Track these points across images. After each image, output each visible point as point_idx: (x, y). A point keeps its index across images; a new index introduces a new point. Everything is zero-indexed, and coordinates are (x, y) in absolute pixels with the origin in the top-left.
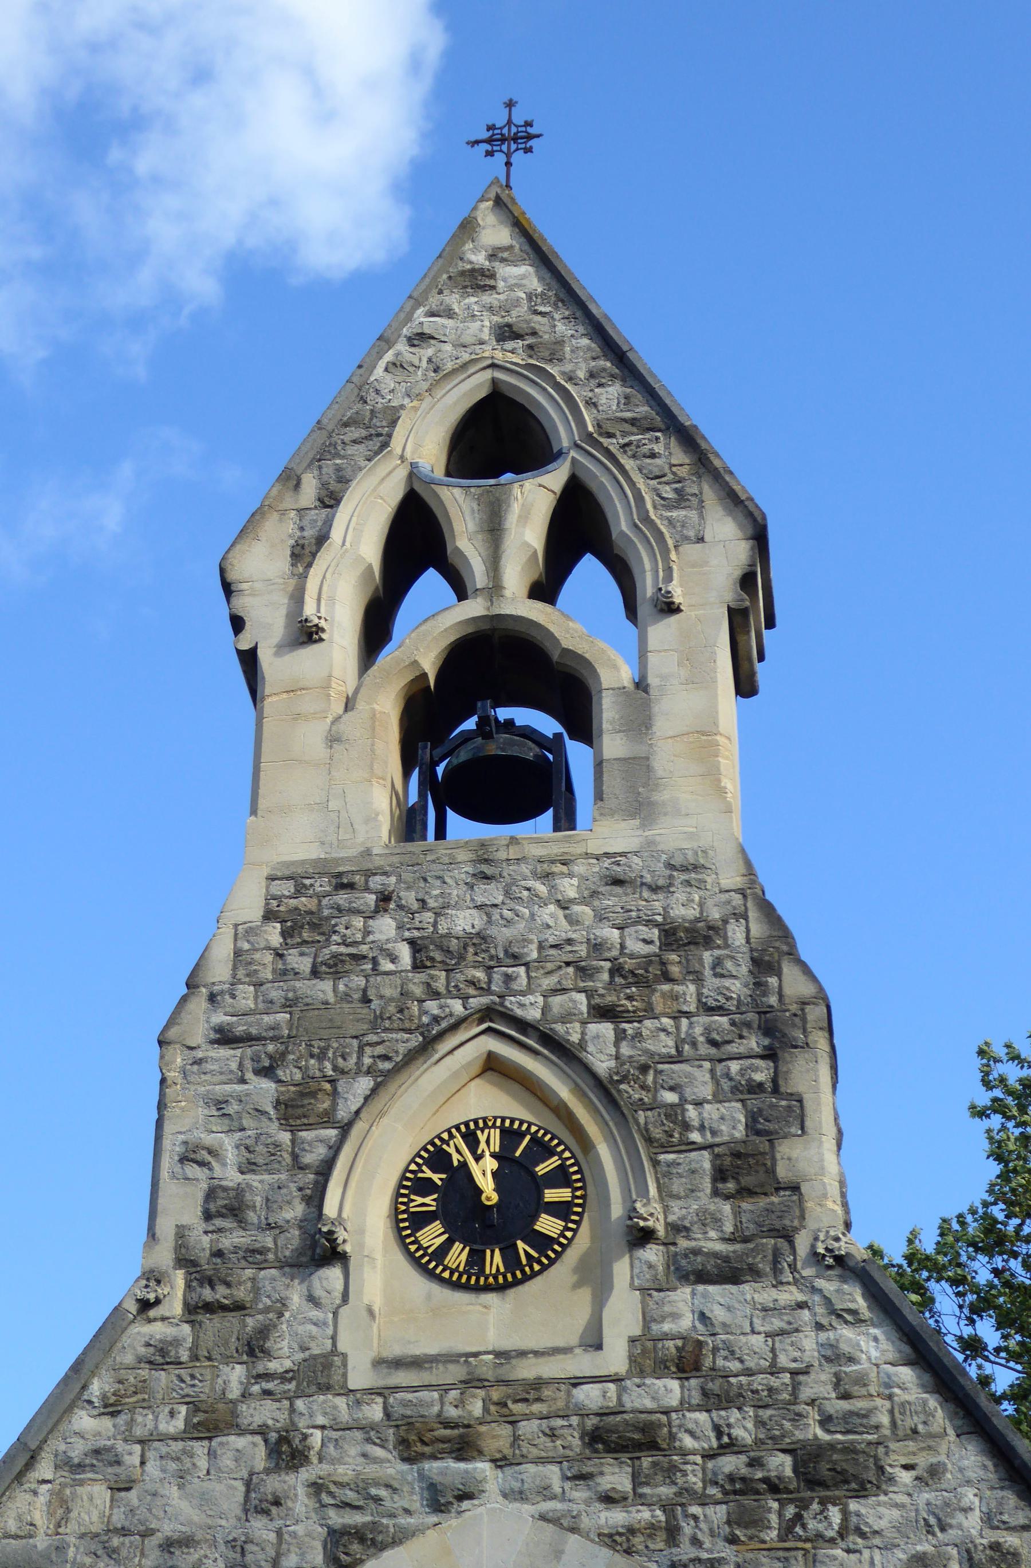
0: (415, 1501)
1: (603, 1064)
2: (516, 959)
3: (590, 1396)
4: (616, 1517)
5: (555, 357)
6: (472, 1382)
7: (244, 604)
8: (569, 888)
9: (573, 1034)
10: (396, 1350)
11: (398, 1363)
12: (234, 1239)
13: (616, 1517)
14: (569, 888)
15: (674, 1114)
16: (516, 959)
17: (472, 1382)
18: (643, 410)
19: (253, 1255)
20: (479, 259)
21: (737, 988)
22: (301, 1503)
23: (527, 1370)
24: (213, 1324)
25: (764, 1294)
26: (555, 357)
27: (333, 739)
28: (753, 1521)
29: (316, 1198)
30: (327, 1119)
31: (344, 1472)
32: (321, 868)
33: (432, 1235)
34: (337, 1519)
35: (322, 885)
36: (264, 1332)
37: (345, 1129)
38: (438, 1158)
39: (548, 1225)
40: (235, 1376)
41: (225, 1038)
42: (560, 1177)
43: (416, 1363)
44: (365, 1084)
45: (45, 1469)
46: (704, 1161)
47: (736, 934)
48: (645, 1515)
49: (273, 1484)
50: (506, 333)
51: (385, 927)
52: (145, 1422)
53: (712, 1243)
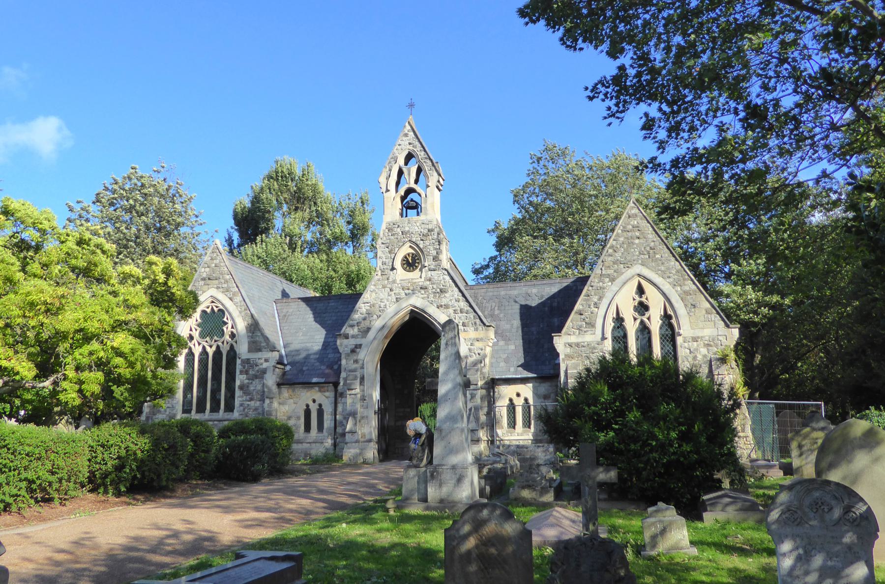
1: (421, 246)
3: (420, 283)
5: (416, 148)
8: (418, 224)
9: (418, 243)
14: (418, 224)
15: (429, 252)
19: (387, 269)
20: (406, 132)
21: (435, 237)
22: (393, 295)
23: (414, 281)
28: (436, 296)
29: (393, 263)
33: (405, 266)
38: (406, 257)
39: (417, 265)
41: (383, 244)
42: (418, 259)
49: (391, 293)
50: (410, 144)
51: (399, 229)
53: (432, 267)
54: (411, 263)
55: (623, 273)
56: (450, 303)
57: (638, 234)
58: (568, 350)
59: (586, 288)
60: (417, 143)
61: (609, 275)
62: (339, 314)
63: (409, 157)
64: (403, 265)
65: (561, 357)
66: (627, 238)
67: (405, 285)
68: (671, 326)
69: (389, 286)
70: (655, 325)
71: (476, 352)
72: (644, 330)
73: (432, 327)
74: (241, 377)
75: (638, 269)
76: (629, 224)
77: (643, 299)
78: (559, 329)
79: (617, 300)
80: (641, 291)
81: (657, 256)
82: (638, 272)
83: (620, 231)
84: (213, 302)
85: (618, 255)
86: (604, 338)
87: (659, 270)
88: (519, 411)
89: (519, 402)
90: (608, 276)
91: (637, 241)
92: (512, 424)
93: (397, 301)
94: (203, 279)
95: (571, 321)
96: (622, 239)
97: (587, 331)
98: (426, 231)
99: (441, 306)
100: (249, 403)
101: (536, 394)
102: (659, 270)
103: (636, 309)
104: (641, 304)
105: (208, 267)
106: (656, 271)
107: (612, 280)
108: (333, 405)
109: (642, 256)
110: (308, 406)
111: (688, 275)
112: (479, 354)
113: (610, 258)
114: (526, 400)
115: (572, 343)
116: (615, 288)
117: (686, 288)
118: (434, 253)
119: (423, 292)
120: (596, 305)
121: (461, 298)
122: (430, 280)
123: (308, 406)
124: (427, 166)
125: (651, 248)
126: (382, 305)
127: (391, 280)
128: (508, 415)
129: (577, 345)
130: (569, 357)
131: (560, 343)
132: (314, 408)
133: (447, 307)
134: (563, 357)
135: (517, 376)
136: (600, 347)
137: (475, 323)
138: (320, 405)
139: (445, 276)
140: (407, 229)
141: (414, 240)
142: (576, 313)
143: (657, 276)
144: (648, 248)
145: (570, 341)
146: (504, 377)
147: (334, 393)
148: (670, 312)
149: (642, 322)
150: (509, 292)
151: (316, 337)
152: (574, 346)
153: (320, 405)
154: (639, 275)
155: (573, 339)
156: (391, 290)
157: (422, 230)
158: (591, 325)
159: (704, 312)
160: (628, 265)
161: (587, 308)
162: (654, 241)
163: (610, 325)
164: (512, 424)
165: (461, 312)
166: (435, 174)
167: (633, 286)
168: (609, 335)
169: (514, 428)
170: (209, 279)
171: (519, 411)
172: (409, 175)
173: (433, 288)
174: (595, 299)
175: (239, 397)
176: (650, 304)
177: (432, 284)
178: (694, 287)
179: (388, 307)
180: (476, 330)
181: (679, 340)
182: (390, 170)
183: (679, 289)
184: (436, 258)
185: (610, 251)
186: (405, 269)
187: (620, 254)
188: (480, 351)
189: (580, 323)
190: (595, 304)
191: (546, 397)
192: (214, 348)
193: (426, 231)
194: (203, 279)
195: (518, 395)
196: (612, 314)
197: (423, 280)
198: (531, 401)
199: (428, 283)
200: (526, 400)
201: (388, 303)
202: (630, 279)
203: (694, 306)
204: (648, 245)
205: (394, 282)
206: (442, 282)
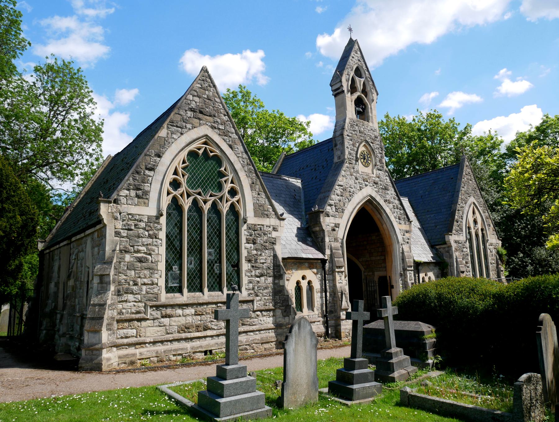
10: (363, 171)
11: (363, 173)
22: (358, 184)
34: (361, 186)
40: (352, 170)
51: (357, 127)
65: (454, 249)
74: (248, 246)
84: (205, 143)
94: (192, 110)
100: (258, 279)
105: (199, 97)
112: (408, 242)
122: (379, 178)
123: (298, 283)
126: (352, 190)
132: (304, 284)
138: (309, 283)
153: (309, 283)
156: (357, 179)
170: (201, 112)
175: (247, 271)
177: (380, 181)
188: (408, 241)
192: (209, 205)
194: (192, 110)
197: (374, 176)
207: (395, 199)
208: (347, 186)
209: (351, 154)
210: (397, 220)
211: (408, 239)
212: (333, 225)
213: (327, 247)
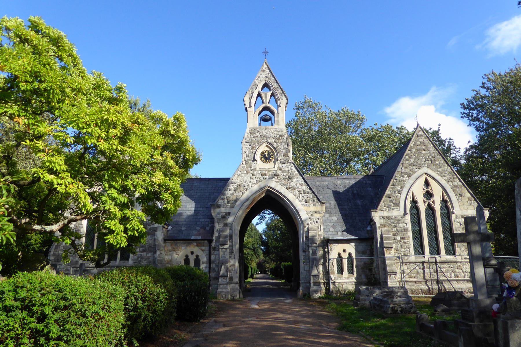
0: (262, 179)
1: (275, 146)
2: (268, 137)
3: (274, 172)
4: (276, 180)
5: (271, 80)
6: (266, 170)
7: (245, 103)
8: (273, 131)
9: (273, 144)
11: (261, 169)
12: (248, 159)
13: (276, 180)
14: (273, 131)
15: (280, 150)
16: (268, 137)
17: (266, 170)
18: (278, 86)
19: (250, 160)
20: (264, 69)
21: (285, 140)
22: (254, 178)
23: (270, 170)
24: (247, 165)
25: (287, 165)
26: (271, 80)
27: (254, 116)
29: (254, 156)
30: (255, 150)
31: (257, 176)
32: (253, 128)
33: (263, 159)
35: (253, 130)
36: (251, 166)
37: (256, 151)
38: (263, 153)
41: (246, 142)
43: (262, 169)
44: (257, 147)
45: (236, 175)
46: (282, 154)
47: (285, 136)
48: (278, 180)
50: (266, 77)
51: (258, 134)
52: (243, 172)
53: (283, 161)
54: (266, 158)
55: (416, 172)
56: (296, 186)
57: (424, 147)
58: (382, 221)
59: (392, 180)
60: (272, 77)
61: (406, 172)
62: (202, 191)
63: (266, 85)
64: (261, 158)
65: (378, 225)
66: (417, 150)
67: (263, 172)
68: (447, 207)
69: (251, 172)
70: (437, 207)
71: (315, 221)
72: (430, 209)
73: (282, 202)
75: (425, 170)
76: (418, 141)
77: (429, 189)
78: (375, 205)
79: (413, 189)
80: (427, 184)
81: (437, 162)
82: (425, 172)
83: (412, 145)
85: (412, 160)
86: (405, 214)
87: (438, 171)
88: (345, 262)
89: (345, 256)
90: (406, 173)
91: (424, 152)
92: (340, 271)
93: (257, 183)
95: (383, 202)
96: (414, 150)
97: (394, 209)
98: (278, 136)
99: (289, 188)
100: (142, 253)
101: (356, 250)
102: (438, 171)
103: (424, 196)
104: (428, 192)
106: (437, 172)
107: (409, 176)
108: (208, 256)
109: (427, 162)
110: (187, 256)
111: (456, 176)
112: (317, 222)
113: (407, 162)
114: (350, 254)
115: (384, 216)
116: (411, 181)
117: (456, 184)
118: (284, 151)
119: (276, 177)
120: (400, 192)
121: (304, 183)
122: (281, 170)
124: (279, 93)
125: (432, 157)
126: (246, 185)
127: (253, 168)
128: (337, 265)
129: (388, 218)
130: (382, 225)
131: (377, 216)
133: (293, 188)
134: (379, 225)
135: (345, 238)
136: (403, 219)
137: (314, 201)
138: (197, 256)
139: (292, 168)
140: (264, 134)
141: (270, 141)
142: (386, 196)
143: (437, 175)
144: (431, 157)
145: (383, 215)
146: (335, 238)
147: (208, 247)
148: (446, 198)
149: (429, 205)
150: (322, 183)
151: (188, 207)
152: (385, 218)
153: (197, 256)
154: (426, 174)
155: (385, 214)
156: (253, 175)
157: (276, 135)
158: (397, 205)
159: (467, 199)
160: (419, 167)
161: (393, 194)
162: (434, 153)
163: (409, 206)
164: (340, 271)
165: (304, 193)
166: (285, 99)
167: (422, 180)
168: (408, 211)
169: (342, 274)
171: (345, 262)
172: (266, 97)
173: (284, 175)
174: (399, 188)
176: (434, 192)
177: (283, 172)
178: (460, 183)
179: (250, 187)
180: (315, 205)
181: (453, 217)
182: (252, 93)
183: (451, 184)
184: (285, 155)
185: (407, 157)
186: (262, 161)
187: (414, 160)
188: (317, 220)
189: (389, 203)
190: (399, 191)
191: (363, 253)
193: (278, 136)
195: (344, 251)
196: (409, 199)
197: (276, 169)
198: (354, 255)
199: (280, 171)
200: (350, 254)
201: (250, 184)
202: (420, 176)
203: (461, 195)
204: (431, 155)
205: (255, 169)
206: (290, 171)
207: (302, 185)
208: (241, 183)
209: (248, 157)
210: (305, 204)
211: (319, 219)
212: (224, 214)
213: (215, 230)
